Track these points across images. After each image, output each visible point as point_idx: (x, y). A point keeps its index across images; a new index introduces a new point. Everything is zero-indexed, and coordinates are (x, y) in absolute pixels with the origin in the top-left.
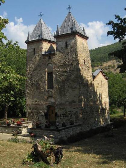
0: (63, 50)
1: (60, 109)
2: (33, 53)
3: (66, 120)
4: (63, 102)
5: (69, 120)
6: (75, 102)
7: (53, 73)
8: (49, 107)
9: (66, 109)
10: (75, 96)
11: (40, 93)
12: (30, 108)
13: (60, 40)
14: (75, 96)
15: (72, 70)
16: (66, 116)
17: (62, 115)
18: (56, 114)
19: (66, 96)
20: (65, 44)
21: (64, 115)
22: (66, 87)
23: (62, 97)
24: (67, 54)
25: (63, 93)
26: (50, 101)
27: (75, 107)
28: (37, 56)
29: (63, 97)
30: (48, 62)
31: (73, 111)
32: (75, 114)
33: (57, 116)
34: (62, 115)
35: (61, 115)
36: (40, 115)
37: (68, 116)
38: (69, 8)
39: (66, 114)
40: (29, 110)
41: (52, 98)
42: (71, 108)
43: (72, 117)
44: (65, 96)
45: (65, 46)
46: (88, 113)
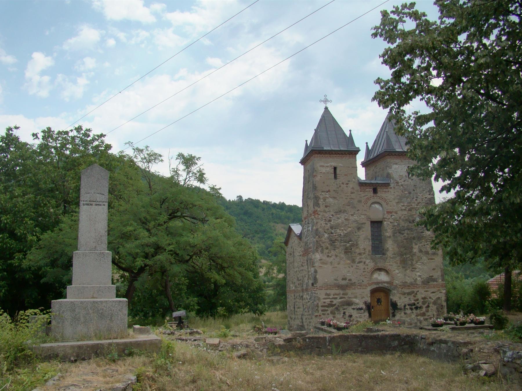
0: (403, 180)
1: (404, 294)
3: (417, 316)
4: (409, 280)
5: (423, 314)
6: (435, 280)
9: (416, 294)
10: (434, 269)
11: (353, 261)
12: (327, 294)
14: (434, 269)
16: (416, 308)
17: (407, 307)
18: (394, 306)
19: (415, 269)
21: (414, 306)
22: (415, 250)
23: (406, 270)
24: (414, 190)
25: (410, 263)
26: (377, 278)
28: (343, 183)
29: (408, 271)
30: (372, 200)
31: (430, 298)
32: (435, 303)
33: (397, 309)
34: (407, 307)
35: (405, 306)
36: (354, 309)
37: (421, 307)
39: (416, 303)
41: (383, 273)
42: (427, 291)
43: (430, 309)
44: (414, 269)
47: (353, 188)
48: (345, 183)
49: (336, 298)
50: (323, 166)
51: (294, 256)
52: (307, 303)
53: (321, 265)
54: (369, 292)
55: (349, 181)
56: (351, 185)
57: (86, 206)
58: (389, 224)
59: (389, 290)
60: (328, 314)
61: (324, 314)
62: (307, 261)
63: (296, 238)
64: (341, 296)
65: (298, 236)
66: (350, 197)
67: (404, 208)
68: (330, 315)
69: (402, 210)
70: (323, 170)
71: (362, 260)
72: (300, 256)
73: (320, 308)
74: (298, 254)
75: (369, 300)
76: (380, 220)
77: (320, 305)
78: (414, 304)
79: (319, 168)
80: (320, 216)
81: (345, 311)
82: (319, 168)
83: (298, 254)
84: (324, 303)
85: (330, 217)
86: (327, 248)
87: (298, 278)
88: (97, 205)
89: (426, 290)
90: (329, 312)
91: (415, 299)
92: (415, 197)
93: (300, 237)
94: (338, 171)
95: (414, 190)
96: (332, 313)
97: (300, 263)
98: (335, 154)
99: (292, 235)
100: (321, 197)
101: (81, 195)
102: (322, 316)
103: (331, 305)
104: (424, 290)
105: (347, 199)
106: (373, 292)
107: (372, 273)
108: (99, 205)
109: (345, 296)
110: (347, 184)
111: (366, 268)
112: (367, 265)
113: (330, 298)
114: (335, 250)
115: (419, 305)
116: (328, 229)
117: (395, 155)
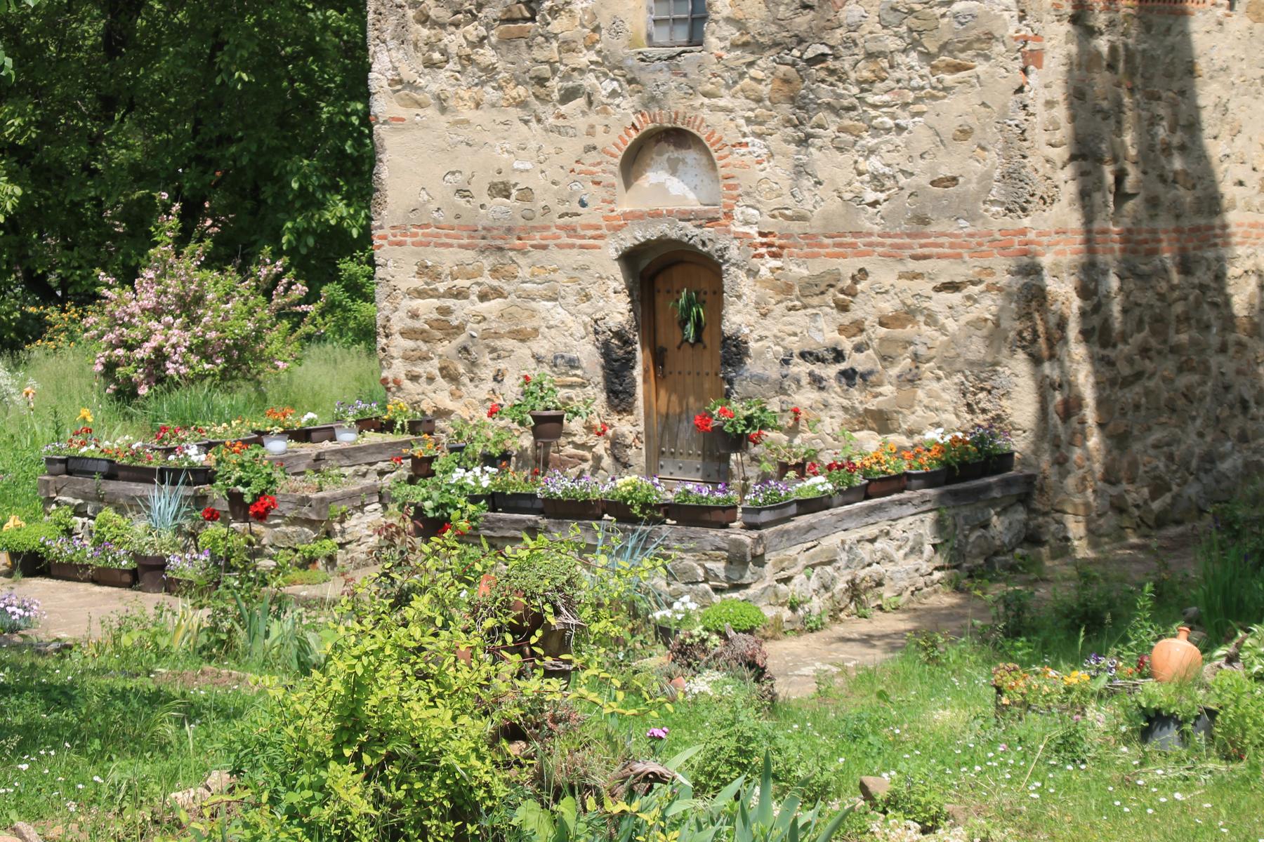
4: (820, 204)
8: (644, 264)
12: (423, 270)
34: (801, 369)
39: (847, 345)
40: (421, 294)
41: (691, 155)
42: (915, 276)
46: (1124, 337)
49: (460, 294)
53: (401, 112)
54: (616, 270)
59: (707, 257)
61: (414, 378)
64: (488, 280)
68: (439, 379)
71: (577, 80)
73: (400, 344)
75: (618, 310)
78: (839, 356)
81: (502, 365)
84: (414, 316)
86: (424, 20)
90: (433, 367)
91: (846, 319)
102: (407, 384)
103: (445, 327)
104: (903, 269)
107: (634, 160)
111: (600, 129)
114: (457, 25)
115: (859, 361)
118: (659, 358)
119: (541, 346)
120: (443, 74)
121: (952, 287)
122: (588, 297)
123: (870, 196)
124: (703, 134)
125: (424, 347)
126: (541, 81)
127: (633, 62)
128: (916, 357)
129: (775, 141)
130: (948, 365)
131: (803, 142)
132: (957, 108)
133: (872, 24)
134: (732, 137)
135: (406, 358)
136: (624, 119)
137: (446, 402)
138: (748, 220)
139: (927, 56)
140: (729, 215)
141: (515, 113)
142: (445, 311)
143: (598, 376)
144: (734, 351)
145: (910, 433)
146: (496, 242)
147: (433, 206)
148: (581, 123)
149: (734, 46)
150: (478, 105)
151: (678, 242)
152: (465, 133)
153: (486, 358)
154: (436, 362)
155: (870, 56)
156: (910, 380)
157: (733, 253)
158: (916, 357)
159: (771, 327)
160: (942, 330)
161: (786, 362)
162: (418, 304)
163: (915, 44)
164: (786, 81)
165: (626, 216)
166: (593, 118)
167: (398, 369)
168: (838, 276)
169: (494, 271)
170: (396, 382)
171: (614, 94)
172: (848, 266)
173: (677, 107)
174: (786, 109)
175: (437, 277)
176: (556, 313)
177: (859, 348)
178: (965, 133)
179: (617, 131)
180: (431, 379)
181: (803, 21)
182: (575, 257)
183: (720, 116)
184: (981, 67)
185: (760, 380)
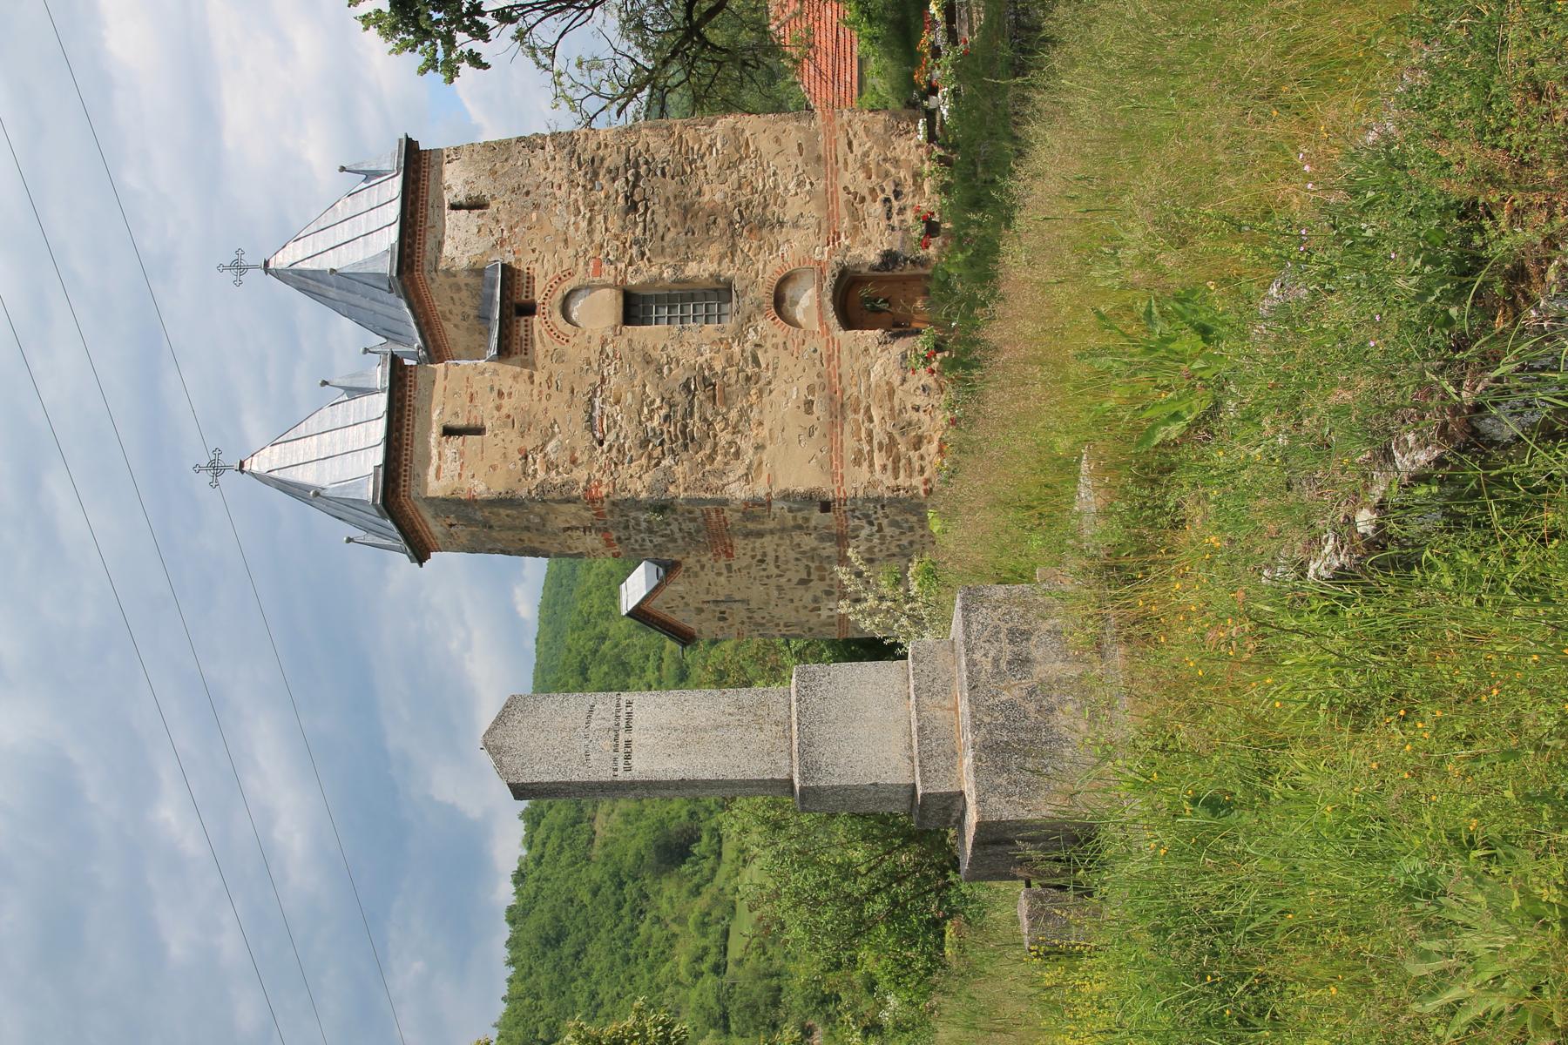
0: (493, 225)
2: (471, 439)
7: (633, 281)
12: (857, 462)
13: (430, 244)
15: (628, 160)
20: (464, 212)
24: (528, 193)
27: (842, 146)
28: (498, 408)
30: (557, 315)
34: (895, 220)
38: (239, 267)
39: (882, 196)
40: (871, 465)
41: (789, 292)
45: (477, 212)
47: (515, 378)
48: (498, 402)
49: (870, 434)
50: (438, 469)
51: (730, 600)
52: (883, 538)
53: (765, 476)
55: (492, 388)
56: (506, 383)
57: (634, 762)
58: (636, 271)
60: (922, 458)
61: (922, 470)
62: (747, 535)
63: (672, 588)
64: (861, 416)
65: (666, 571)
66: (545, 386)
67: (584, 225)
69: (590, 232)
70: (451, 467)
71: (748, 354)
72: (729, 567)
73: (903, 480)
74: (722, 579)
76: (621, 299)
77: (891, 482)
78: (887, 200)
79: (443, 482)
80: (605, 480)
81: (909, 406)
82: (443, 482)
83: (722, 579)
84: (884, 467)
85: (610, 450)
86: (711, 458)
87: (802, 582)
88: (629, 728)
89: (841, 164)
90: (914, 455)
91: (869, 198)
92: (549, 191)
93: (669, 569)
94: (460, 422)
95: (528, 193)
96: (917, 444)
97: (753, 571)
98: (399, 430)
99: (658, 607)
100: (541, 475)
101: (594, 779)
102: (926, 475)
103: (890, 446)
105: (549, 397)
106: (848, 320)
107: (793, 323)
108: (628, 720)
109: (863, 405)
110: (500, 394)
112: (764, 337)
113: (871, 452)
116: (650, 457)
117: (410, 246)
118: (897, 325)
119: (896, 380)
120: (743, 445)
121: (850, 144)
122: (866, 350)
123: (808, 187)
124: (777, 277)
125: (903, 461)
126: (748, 379)
127: (739, 317)
128: (885, 160)
129: (781, 239)
130: (887, 144)
131: (782, 224)
132: (765, 145)
133: (725, 187)
134: (779, 261)
135: (911, 476)
136: (766, 324)
137: (934, 447)
138: (822, 253)
139: (741, 159)
140: (819, 262)
141: (765, 399)
142: (880, 444)
143: (911, 339)
144: (890, 258)
145: (922, 162)
146: (839, 409)
147: (819, 455)
148: (771, 353)
149: (732, 261)
150: (761, 424)
151: (835, 292)
152: (777, 433)
153: (906, 416)
154: (911, 453)
155: (740, 187)
156: (896, 162)
157: (838, 259)
158: (885, 160)
159: (875, 237)
160: (871, 148)
161: (893, 229)
162: (877, 467)
163: (735, 166)
164: (751, 231)
165: (821, 324)
166: (768, 345)
167: (917, 481)
168: (848, 201)
169: (856, 411)
170: (927, 482)
171: (756, 331)
172: (842, 196)
173: (763, 293)
174: (765, 232)
175: (860, 451)
176: (877, 370)
177: (883, 191)
178: (777, 140)
179: (776, 330)
180: (922, 458)
181: (722, 222)
182: (845, 355)
183: (768, 269)
184: (747, 133)
185: (903, 242)
